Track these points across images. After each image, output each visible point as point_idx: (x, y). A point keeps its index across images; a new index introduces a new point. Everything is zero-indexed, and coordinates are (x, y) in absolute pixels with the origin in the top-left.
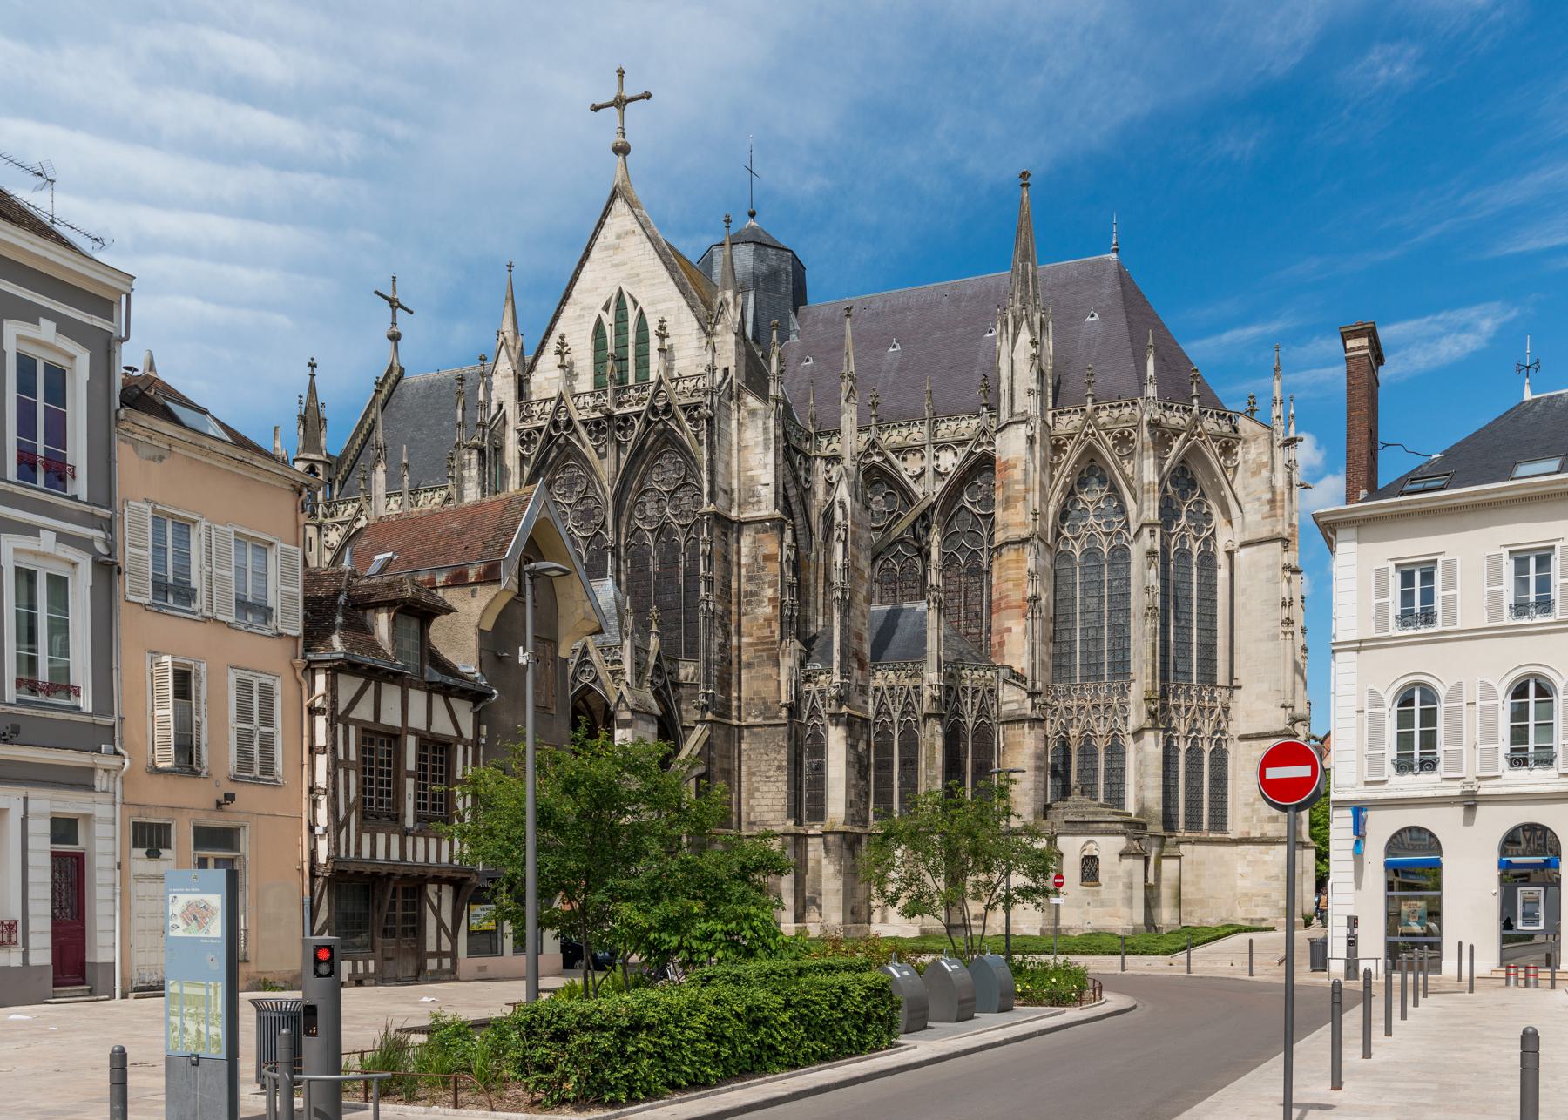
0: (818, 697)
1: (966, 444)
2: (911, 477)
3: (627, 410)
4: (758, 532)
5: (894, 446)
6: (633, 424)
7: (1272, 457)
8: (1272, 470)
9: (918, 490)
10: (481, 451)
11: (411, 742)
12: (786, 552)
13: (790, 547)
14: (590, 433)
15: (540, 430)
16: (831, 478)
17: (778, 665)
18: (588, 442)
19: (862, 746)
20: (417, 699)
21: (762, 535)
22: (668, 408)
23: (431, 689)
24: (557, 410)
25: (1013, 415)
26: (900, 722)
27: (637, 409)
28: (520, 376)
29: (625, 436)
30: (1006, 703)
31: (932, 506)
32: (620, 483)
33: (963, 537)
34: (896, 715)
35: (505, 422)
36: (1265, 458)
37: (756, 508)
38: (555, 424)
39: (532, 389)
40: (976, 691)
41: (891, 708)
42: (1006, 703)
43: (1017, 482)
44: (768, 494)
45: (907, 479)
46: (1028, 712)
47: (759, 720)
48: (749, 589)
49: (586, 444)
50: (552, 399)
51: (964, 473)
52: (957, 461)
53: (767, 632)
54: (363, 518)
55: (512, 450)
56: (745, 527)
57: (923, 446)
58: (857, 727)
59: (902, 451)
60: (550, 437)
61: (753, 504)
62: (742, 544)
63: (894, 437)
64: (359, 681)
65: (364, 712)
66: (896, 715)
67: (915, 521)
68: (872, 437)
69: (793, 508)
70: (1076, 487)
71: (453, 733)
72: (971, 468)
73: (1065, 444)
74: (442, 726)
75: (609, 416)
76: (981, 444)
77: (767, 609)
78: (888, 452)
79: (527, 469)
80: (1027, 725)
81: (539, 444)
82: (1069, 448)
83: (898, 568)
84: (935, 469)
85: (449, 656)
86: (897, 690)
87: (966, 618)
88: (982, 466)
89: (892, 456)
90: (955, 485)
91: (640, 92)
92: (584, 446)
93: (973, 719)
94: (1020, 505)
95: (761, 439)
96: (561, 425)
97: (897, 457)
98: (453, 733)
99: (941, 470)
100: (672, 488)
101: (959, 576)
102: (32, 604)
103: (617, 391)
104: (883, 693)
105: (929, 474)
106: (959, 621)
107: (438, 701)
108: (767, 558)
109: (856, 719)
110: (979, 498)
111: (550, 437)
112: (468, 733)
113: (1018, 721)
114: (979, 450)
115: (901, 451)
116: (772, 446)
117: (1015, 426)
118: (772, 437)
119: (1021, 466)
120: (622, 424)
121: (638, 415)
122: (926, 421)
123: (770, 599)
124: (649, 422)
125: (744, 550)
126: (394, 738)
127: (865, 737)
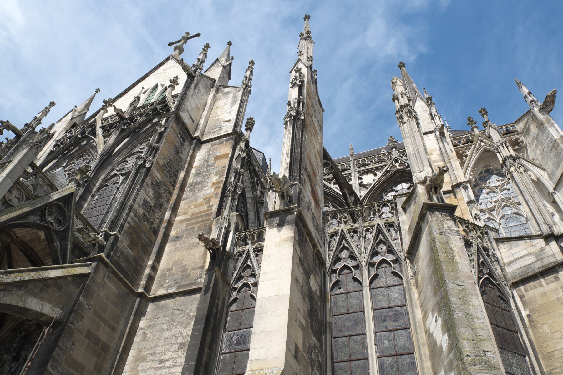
0: (252, 255)
51: (383, 182)
53: (205, 208)
69: (248, 206)
72: (388, 179)
90: (376, 190)
91: (196, 33)
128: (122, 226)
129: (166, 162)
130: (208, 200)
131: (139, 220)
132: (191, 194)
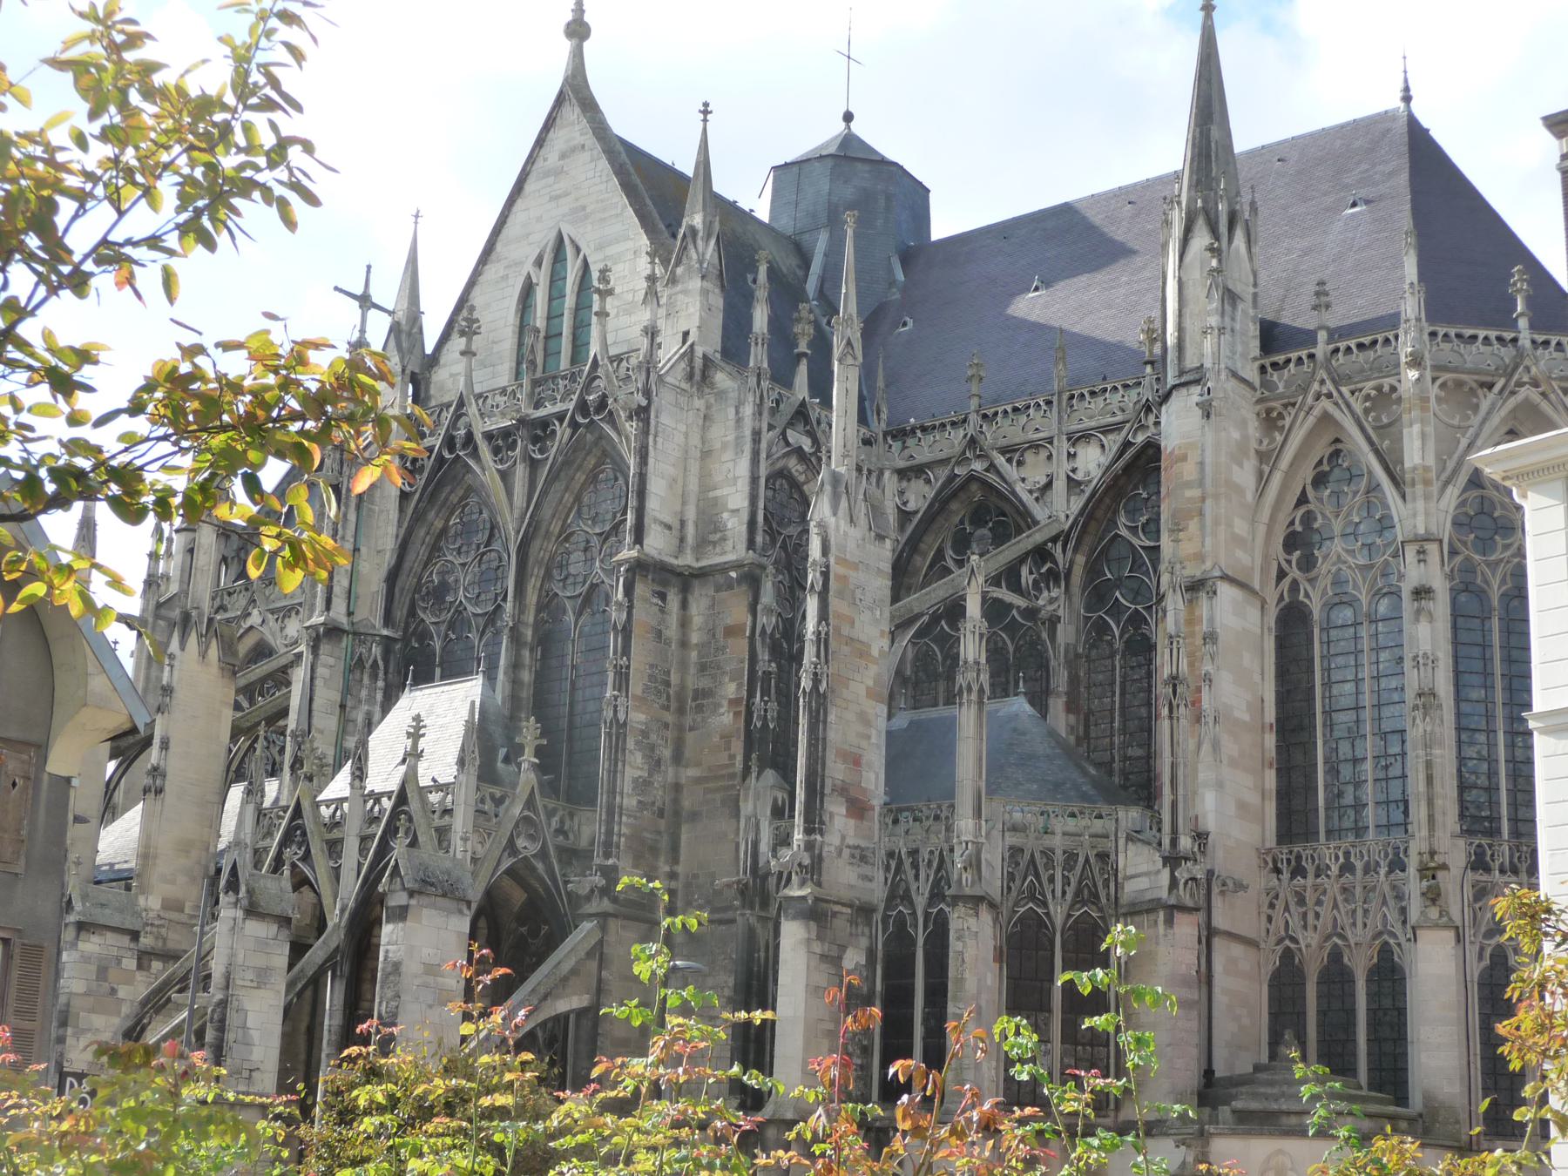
1: (1120, 429)
2: (1031, 492)
3: (548, 409)
5: (1002, 442)
6: (554, 432)
9: (1039, 512)
12: (762, 620)
13: (769, 611)
14: (496, 451)
16: (905, 504)
18: (492, 464)
19: (853, 958)
21: (724, 594)
24: (458, 416)
25: (1182, 373)
26: (927, 915)
27: (559, 407)
28: (413, 374)
29: (542, 451)
30: (1132, 877)
31: (1062, 537)
32: (529, 525)
33: (1118, 587)
34: (920, 902)
37: (718, 550)
38: (450, 442)
39: (432, 392)
40: (1071, 857)
41: (913, 887)
42: (1132, 877)
43: (1188, 485)
44: (736, 526)
45: (1025, 497)
46: (1164, 894)
48: (701, 686)
49: (486, 469)
50: (448, 405)
51: (1116, 478)
52: (1105, 460)
53: (723, 758)
54: (255, 612)
56: (696, 583)
57: (1050, 441)
58: (841, 925)
60: (441, 460)
61: (714, 544)
63: (1012, 430)
66: (920, 902)
67: (1021, 560)
68: (970, 431)
70: (1309, 489)
73: (1281, 416)
76: (1143, 427)
77: (725, 718)
78: (995, 454)
80: (1161, 914)
81: (425, 474)
82: (1287, 422)
83: (1011, 648)
84: (1068, 477)
86: (924, 854)
87: (1123, 731)
89: (1000, 460)
90: (1100, 500)
92: (483, 469)
93: (1066, 907)
94: (1193, 526)
95: (731, 438)
96: (460, 444)
97: (1009, 461)
99: (1079, 476)
100: (607, 528)
101: (1112, 656)
104: (900, 863)
105: (1060, 485)
106: (1112, 735)
108: (731, 631)
109: (837, 908)
110: (1143, 519)
113: (1148, 911)
114: (1140, 438)
115: (1015, 451)
116: (748, 447)
117: (1184, 391)
118: (748, 432)
119: (1193, 458)
120: (539, 432)
121: (561, 417)
122: (1055, 399)
124: (574, 425)
128: (618, 847)
129: (646, 680)
130: (726, 738)
131: (635, 818)
132: (699, 718)
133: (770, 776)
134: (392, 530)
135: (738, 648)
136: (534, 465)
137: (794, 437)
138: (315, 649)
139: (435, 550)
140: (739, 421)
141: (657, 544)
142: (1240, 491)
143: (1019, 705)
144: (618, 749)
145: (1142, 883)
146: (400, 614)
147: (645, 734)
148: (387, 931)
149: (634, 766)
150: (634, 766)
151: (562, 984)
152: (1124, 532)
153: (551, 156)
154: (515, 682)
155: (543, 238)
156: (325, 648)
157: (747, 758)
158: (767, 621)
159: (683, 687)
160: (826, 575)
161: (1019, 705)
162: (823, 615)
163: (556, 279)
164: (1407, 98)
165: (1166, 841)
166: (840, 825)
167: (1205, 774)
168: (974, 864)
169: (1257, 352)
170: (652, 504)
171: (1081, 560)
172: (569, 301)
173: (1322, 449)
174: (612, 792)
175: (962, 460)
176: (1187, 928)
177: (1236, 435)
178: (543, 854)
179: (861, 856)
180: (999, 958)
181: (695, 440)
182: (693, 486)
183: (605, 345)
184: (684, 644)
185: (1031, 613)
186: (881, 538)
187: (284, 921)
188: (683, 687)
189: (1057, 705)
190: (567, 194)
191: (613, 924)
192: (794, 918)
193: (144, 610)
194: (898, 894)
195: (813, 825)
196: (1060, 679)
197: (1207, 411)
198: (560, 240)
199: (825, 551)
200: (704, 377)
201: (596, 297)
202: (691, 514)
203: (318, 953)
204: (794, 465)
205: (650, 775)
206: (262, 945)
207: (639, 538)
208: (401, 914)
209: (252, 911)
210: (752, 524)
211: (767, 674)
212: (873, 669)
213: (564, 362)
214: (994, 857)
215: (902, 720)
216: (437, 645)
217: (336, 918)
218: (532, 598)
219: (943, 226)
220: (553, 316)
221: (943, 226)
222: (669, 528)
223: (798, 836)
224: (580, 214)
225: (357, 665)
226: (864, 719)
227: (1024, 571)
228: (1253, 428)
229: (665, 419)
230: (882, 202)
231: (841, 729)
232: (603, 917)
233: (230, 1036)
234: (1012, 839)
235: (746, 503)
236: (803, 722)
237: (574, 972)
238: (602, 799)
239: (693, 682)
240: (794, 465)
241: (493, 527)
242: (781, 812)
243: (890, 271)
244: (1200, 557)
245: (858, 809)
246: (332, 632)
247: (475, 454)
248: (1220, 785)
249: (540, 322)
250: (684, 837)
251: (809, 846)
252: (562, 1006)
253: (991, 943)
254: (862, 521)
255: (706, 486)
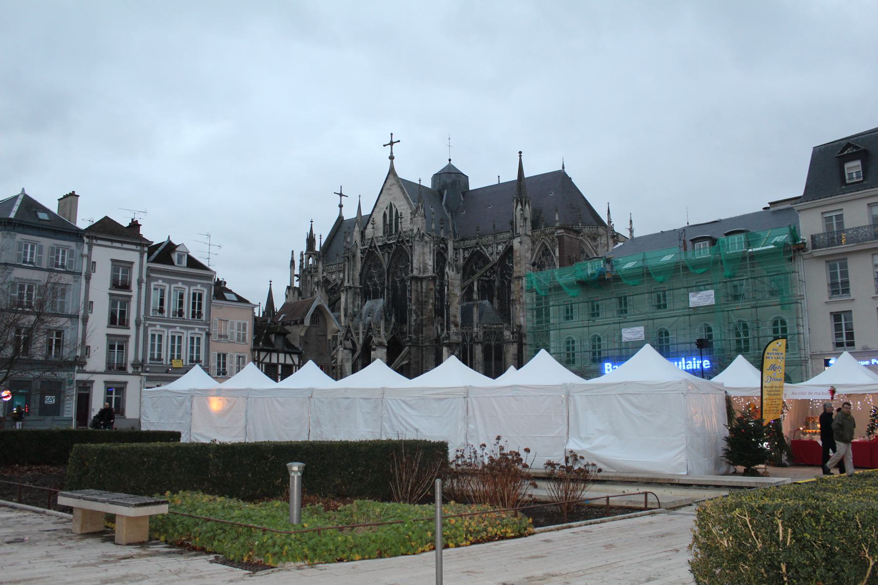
3: (391, 242)
4: (428, 281)
7: (608, 242)
8: (608, 246)
9: (491, 259)
10: (348, 258)
11: (280, 367)
12: (437, 287)
13: (438, 286)
14: (381, 250)
15: (366, 249)
17: (434, 325)
20: (282, 356)
22: (402, 241)
23: (285, 353)
24: (372, 242)
31: (495, 264)
35: (357, 247)
36: (606, 242)
38: (371, 247)
43: (518, 257)
44: (430, 268)
45: (488, 256)
47: (429, 344)
49: (379, 253)
55: (359, 255)
59: (487, 246)
60: (369, 251)
62: (423, 285)
64: (265, 353)
65: (267, 360)
71: (292, 363)
72: (507, 251)
74: (289, 361)
75: (386, 244)
77: (431, 307)
79: (363, 261)
85: (292, 343)
86: (469, 333)
88: (510, 250)
89: (483, 247)
98: (292, 363)
102: (193, 344)
103: (388, 236)
105: (495, 253)
107: (288, 356)
108: (431, 289)
111: (369, 251)
112: (297, 362)
121: (394, 243)
123: (432, 304)
125: (424, 287)
126: (275, 366)
127: (458, 350)
130: (431, 311)
133: (440, 318)
134: (360, 265)
135: (432, 293)
136: (389, 253)
137: (441, 245)
138: (347, 291)
139: (369, 269)
140: (430, 247)
141: (415, 273)
142: (528, 258)
143: (486, 302)
144: (411, 314)
145: (508, 337)
146: (363, 282)
147: (415, 310)
148: (372, 353)
149: (414, 317)
150: (414, 317)
151: (403, 360)
152: (507, 263)
153: (388, 186)
154: (388, 298)
155: (387, 203)
156: (349, 291)
157: (435, 315)
158: (438, 288)
159: (422, 300)
160: (448, 282)
161: (486, 302)
162: (448, 290)
163: (391, 212)
164: (563, 168)
165: (512, 330)
166: (453, 329)
167: (521, 314)
168: (477, 336)
169: (531, 229)
170: (414, 265)
171: (499, 269)
172: (394, 218)
173: (543, 248)
174: (410, 322)
175: (476, 247)
176: (515, 346)
177: (526, 247)
178: (397, 334)
179: (457, 334)
180: (482, 351)
181: (421, 250)
182: (421, 260)
183: (402, 228)
184: (422, 292)
185: (490, 281)
186: (458, 273)
187: (350, 349)
188: (422, 300)
189: (495, 301)
190: (391, 194)
191: (412, 347)
192: (446, 346)
193: (300, 273)
194: (464, 340)
195: (448, 329)
196: (496, 293)
197: (520, 243)
198: (391, 203)
199: (448, 278)
200: (423, 237)
201: (399, 219)
202: (422, 266)
203: (357, 355)
204: (442, 251)
205: (417, 318)
206: (347, 354)
207: (412, 271)
208: (374, 350)
209: (345, 348)
210: (434, 268)
211: (438, 298)
212: (458, 299)
213: (394, 232)
214: (481, 334)
215: (465, 304)
216: (371, 289)
217: (359, 347)
218: (390, 280)
219: (472, 187)
220: (391, 220)
221: (472, 187)
222: (417, 269)
223: (445, 331)
224: (395, 199)
225: (355, 293)
226: (457, 308)
227: (488, 273)
228: (530, 245)
229: (416, 247)
230: (458, 182)
231: (452, 310)
232: (410, 346)
233: (343, 371)
234: (485, 330)
235: (432, 264)
236: (445, 310)
237: (405, 356)
238: (408, 324)
239: (424, 299)
240: (442, 251)
241: (381, 264)
242: (442, 325)
243: (460, 198)
244: (520, 272)
245: (456, 325)
246: (350, 288)
247: (376, 250)
248: (523, 316)
249: (388, 222)
250: (424, 329)
251: (447, 333)
252: (404, 363)
253: (481, 350)
254: (455, 270)
255: (424, 260)
